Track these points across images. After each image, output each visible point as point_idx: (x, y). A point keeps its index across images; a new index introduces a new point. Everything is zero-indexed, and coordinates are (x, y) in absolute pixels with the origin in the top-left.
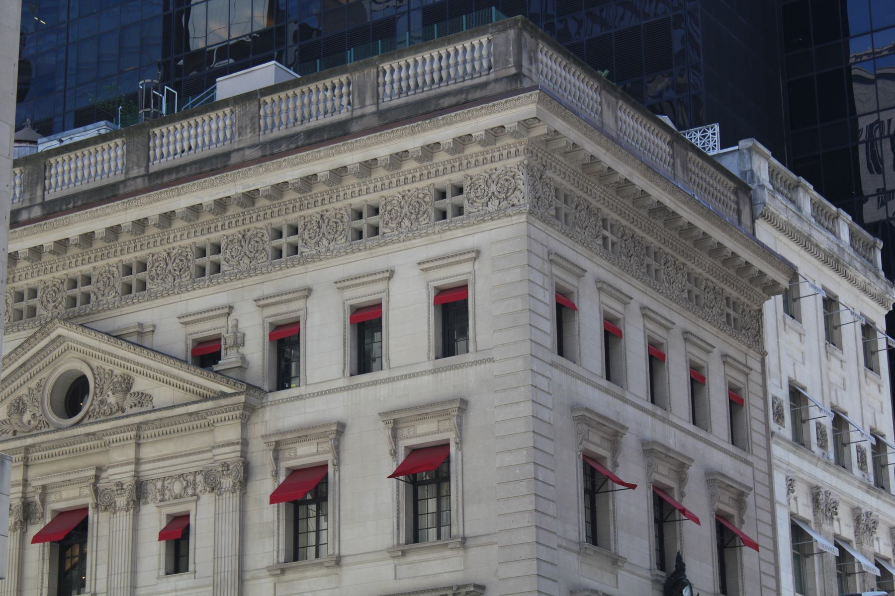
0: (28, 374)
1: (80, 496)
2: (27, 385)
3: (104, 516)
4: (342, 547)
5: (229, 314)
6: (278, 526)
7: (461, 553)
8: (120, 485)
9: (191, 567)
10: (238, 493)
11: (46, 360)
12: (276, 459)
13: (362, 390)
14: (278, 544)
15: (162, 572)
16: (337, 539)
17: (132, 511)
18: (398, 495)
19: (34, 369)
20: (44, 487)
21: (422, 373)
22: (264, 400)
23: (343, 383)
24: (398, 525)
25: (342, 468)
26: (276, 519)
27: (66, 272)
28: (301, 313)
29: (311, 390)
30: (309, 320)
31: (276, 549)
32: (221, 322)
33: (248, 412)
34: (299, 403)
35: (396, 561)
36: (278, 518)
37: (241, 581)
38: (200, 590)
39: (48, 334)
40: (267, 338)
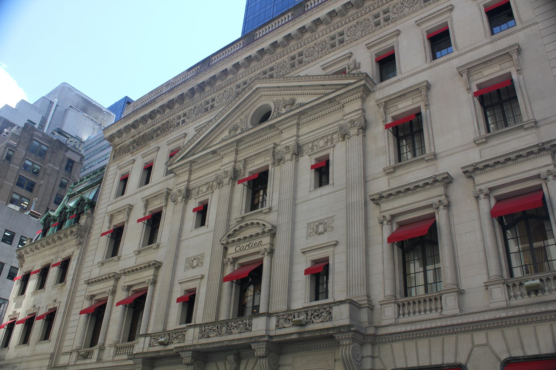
0: (240, 112)
1: (265, 162)
3: (277, 168)
4: (436, 149)
5: (350, 57)
6: (389, 147)
7: (534, 131)
8: (287, 147)
9: (331, 182)
10: (361, 135)
11: (250, 103)
12: (385, 112)
13: (440, 66)
14: (390, 157)
15: (312, 188)
16: (432, 145)
17: (294, 160)
18: (476, 110)
19: (244, 109)
20: (245, 160)
21: (483, 46)
22: (375, 88)
23: (428, 65)
24: (478, 127)
25: (431, 108)
26: (387, 144)
27: (262, 69)
28: (395, 44)
29: (404, 76)
30: (400, 46)
31: (388, 159)
32: (346, 62)
33: (367, 91)
34: (398, 84)
35: (480, 147)
36: (388, 143)
37: (366, 182)
38: (337, 193)
40: (374, 61)
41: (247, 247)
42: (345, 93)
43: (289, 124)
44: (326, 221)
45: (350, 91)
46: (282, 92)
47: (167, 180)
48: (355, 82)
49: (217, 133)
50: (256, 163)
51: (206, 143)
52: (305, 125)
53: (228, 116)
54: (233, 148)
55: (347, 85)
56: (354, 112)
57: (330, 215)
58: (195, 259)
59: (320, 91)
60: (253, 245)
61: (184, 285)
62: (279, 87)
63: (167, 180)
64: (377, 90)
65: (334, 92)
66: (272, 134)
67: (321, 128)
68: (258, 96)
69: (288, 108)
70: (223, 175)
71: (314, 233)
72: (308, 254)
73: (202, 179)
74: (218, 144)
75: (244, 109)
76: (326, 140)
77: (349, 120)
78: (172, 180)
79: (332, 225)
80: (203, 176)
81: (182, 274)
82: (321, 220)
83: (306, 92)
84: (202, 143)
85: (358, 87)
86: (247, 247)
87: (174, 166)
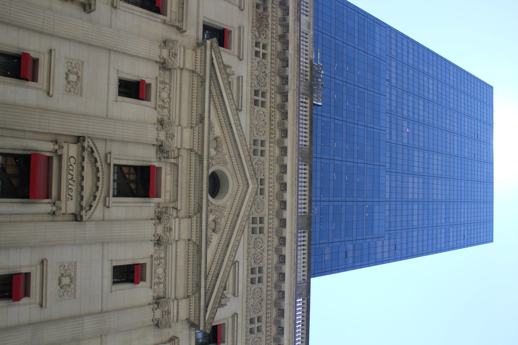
2: (228, 154)
19: (234, 161)
39: (251, 178)
41: (70, 177)
42: (200, 306)
43: (194, 230)
44: (73, 286)
45: (200, 311)
46: (231, 216)
47: (198, 24)
48: (205, 320)
49: (222, 120)
50: (169, 177)
51: (217, 102)
52: (187, 246)
53: (235, 141)
54: (198, 70)
55: (206, 306)
56: (178, 313)
57: (78, 292)
58: (78, 77)
59: (213, 268)
60: (70, 186)
61: (47, 57)
62: (238, 216)
63: (198, 24)
64: (190, 331)
65: (205, 287)
66: (193, 203)
67: (176, 266)
68: (240, 182)
69: (212, 225)
70: (173, 51)
71: (63, 272)
72: (39, 268)
73: (178, 86)
74: (209, 117)
75: (234, 161)
76: (161, 277)
77: (172, 312)
78: (194, 34)
79: (66, 296)
80: (180, 94)
81: (65, 52)
82: (75, 280)
83: (219, 250)
84: (220, 96)
85: (199, 320)
86: (70, 177)
87: (208, 53)
